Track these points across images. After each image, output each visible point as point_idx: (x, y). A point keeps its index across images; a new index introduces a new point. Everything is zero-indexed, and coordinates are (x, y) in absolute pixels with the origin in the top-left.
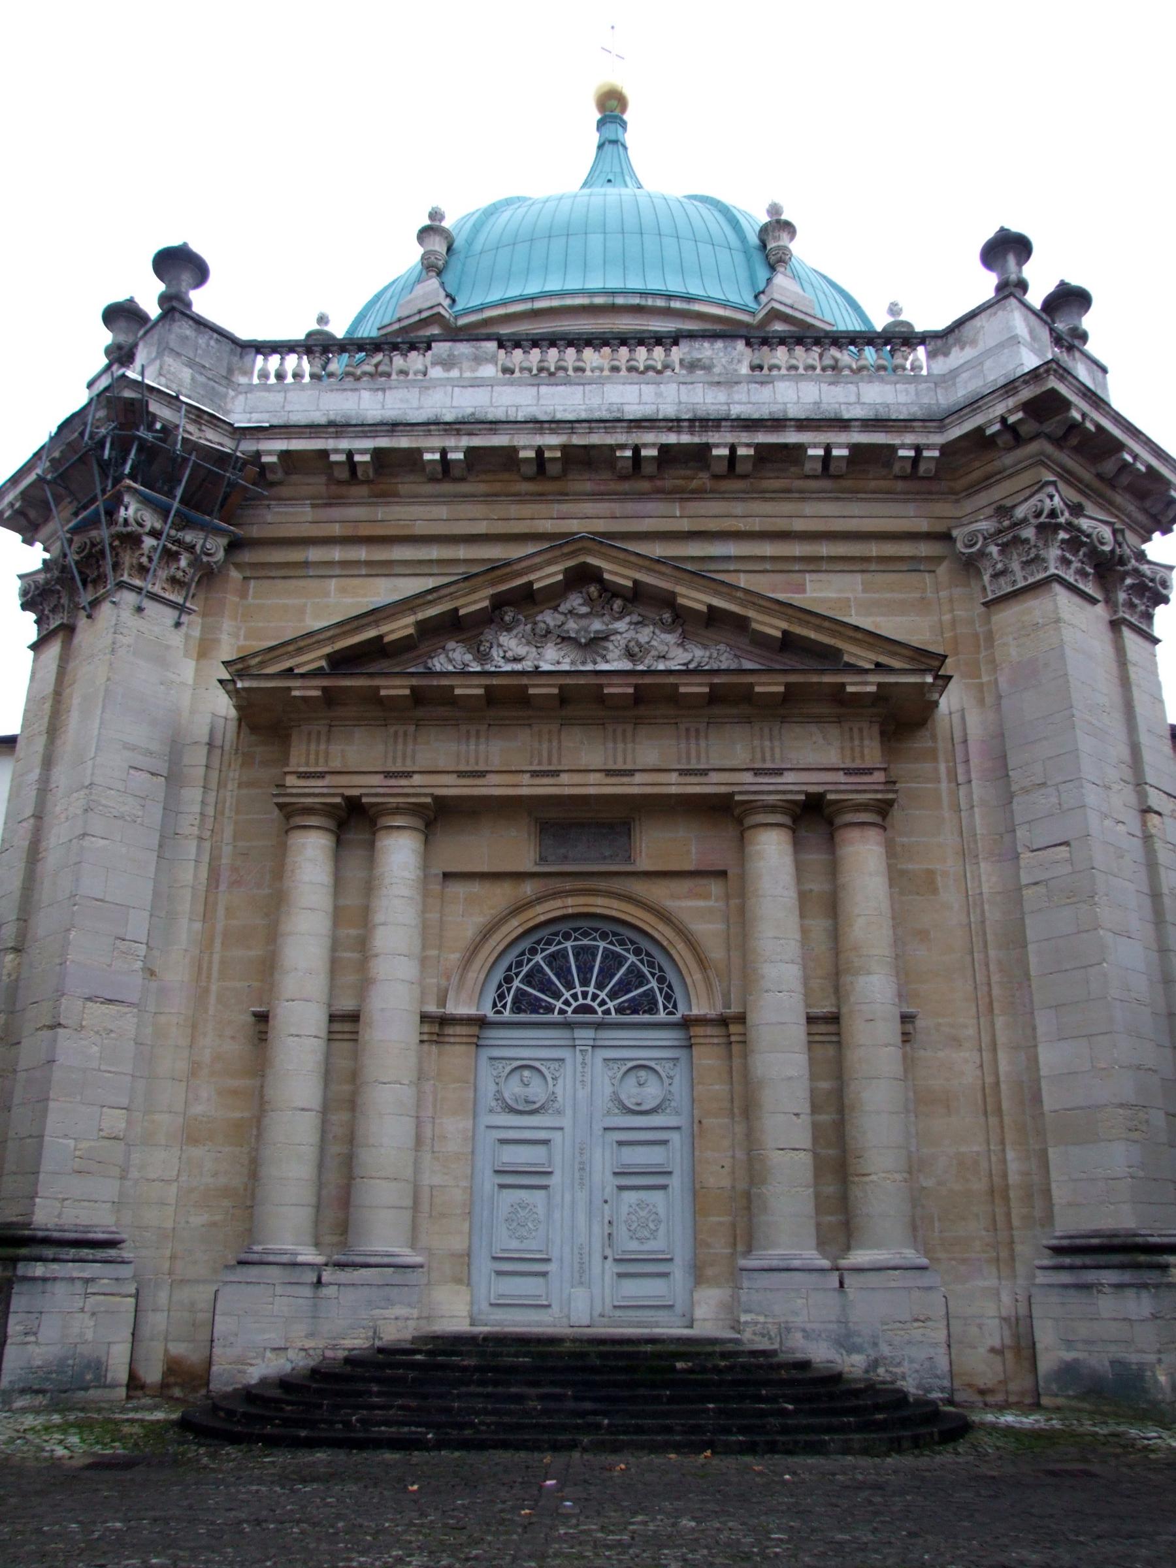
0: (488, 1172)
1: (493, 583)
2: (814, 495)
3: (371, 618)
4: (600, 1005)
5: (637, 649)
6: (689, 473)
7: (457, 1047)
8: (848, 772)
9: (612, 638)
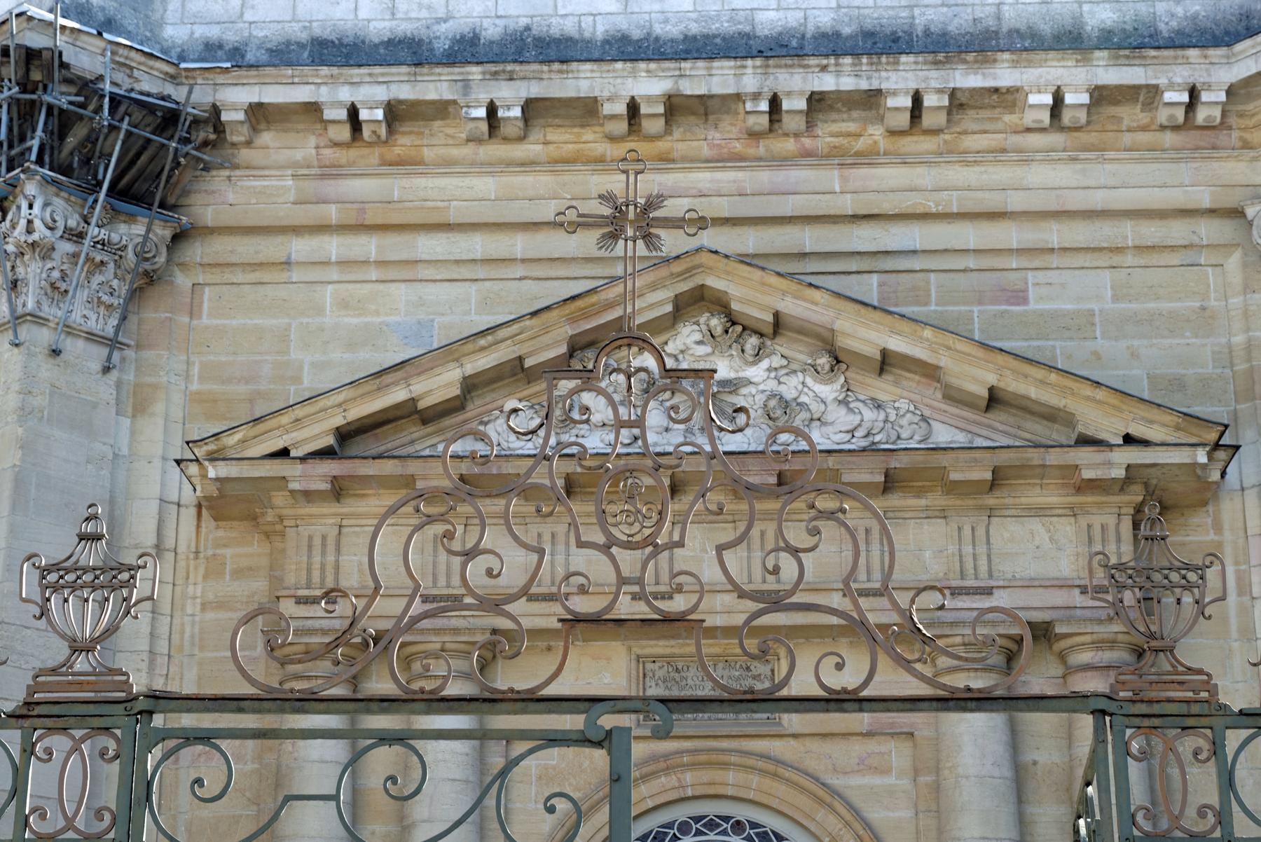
1: (573, 320)
2: (1039, 156)
3: (399, 374)
5: (779, 412)
6: (852, 127)
8: (1084, 590)
9: (744, 391)
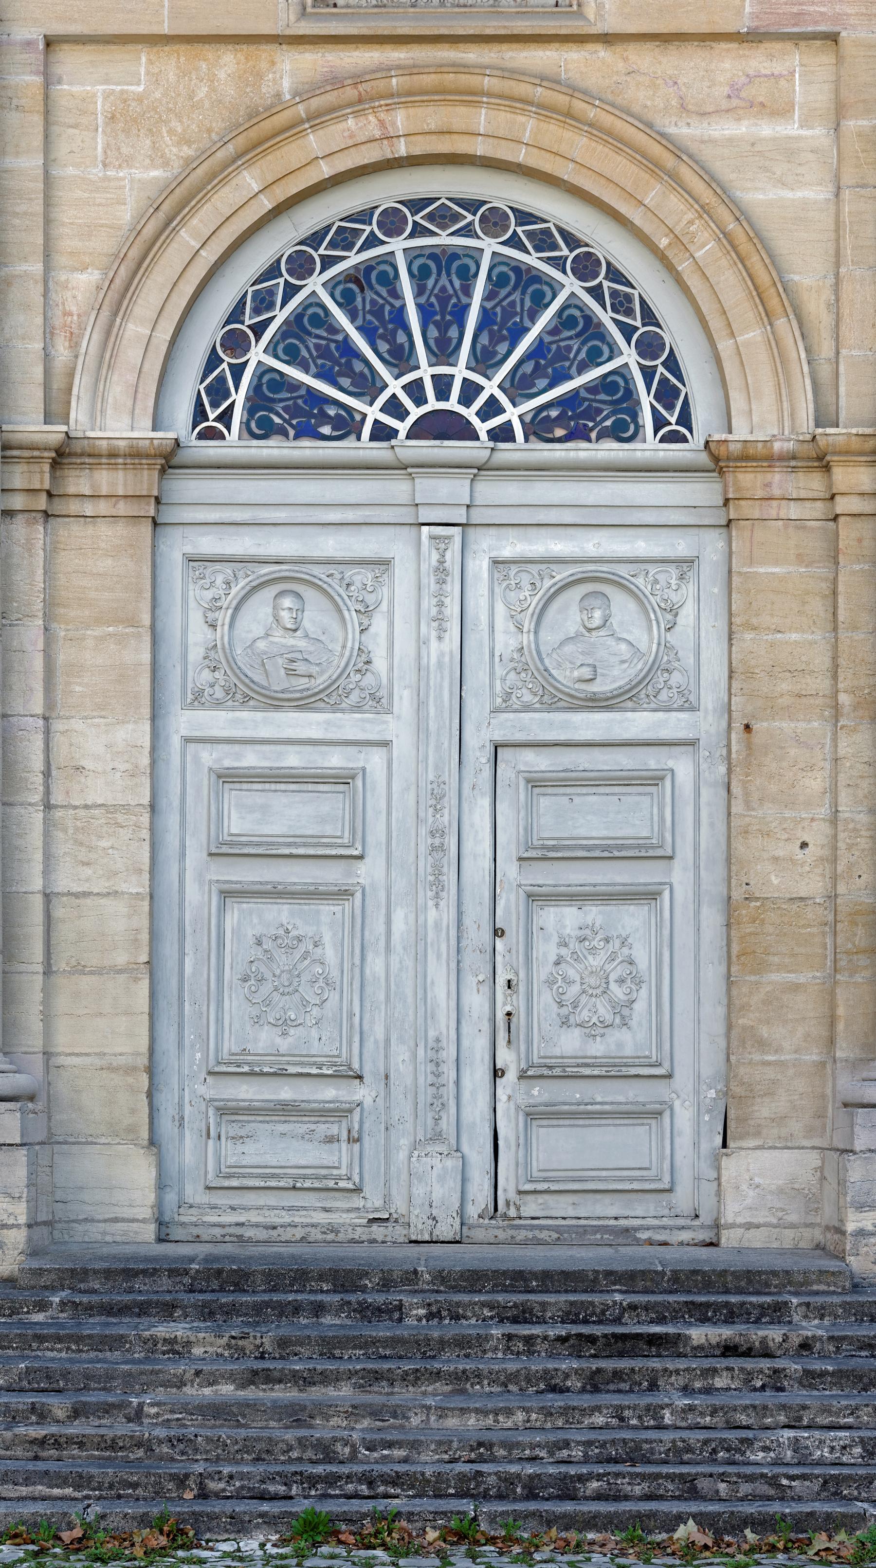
0: (195, 856)
4: (485, 414)
7: (107, 533)
